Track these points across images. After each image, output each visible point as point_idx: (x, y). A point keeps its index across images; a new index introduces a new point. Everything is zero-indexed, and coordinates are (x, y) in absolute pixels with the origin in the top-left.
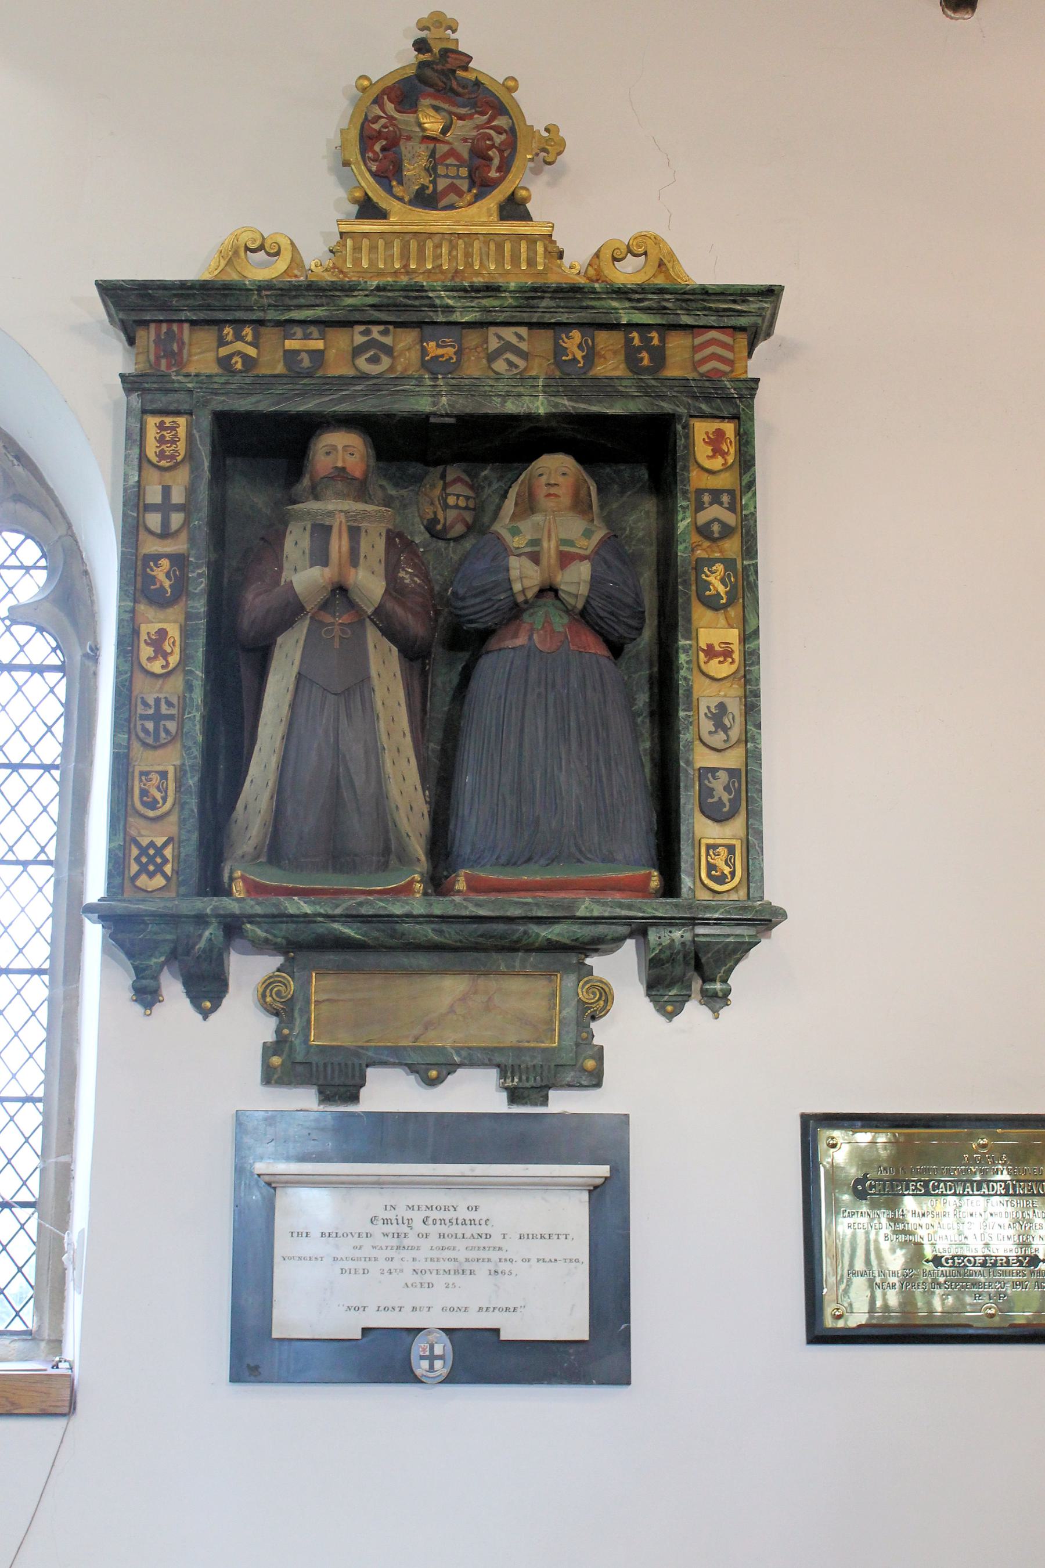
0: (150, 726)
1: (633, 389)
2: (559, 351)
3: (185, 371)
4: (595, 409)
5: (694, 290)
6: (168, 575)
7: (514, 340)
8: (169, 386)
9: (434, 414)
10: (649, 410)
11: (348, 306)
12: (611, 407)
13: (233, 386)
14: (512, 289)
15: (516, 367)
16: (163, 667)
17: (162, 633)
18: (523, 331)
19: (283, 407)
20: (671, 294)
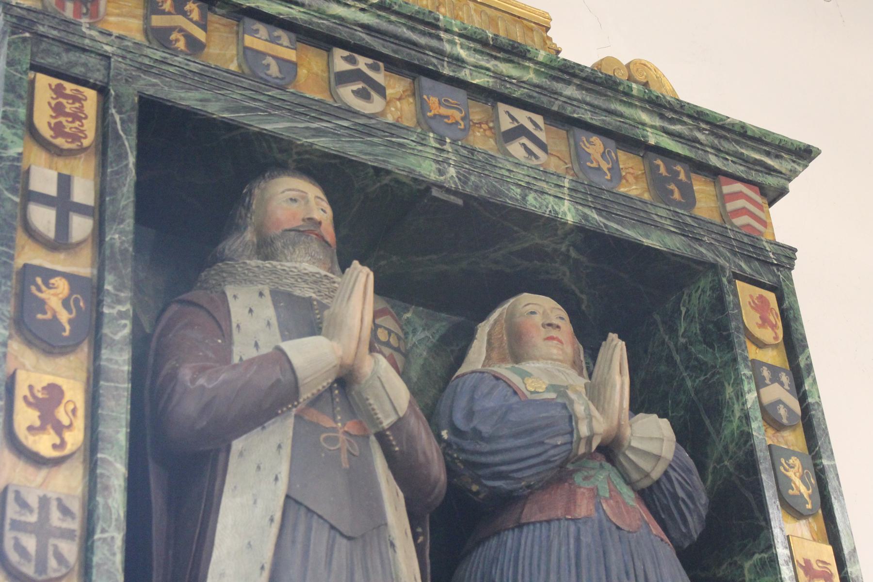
0: (30, 543)
1: (668, 222)
2: (579, 156)
3: (100, 26)
4: (631, 233)
5: (733, 125)
6: (66, 303)
7: (530, 127)
8: (75, 40)
9: (440, 187)
10: (688, 253)
11: (334, 17)
12: (648, 237)
13: (171, 69)
14: (541, 58)
15: (537, 157)
16: (55, 446)
17: (55, 393)
18: (539, 119)
19: (241, 117)
20: (708, 123)
